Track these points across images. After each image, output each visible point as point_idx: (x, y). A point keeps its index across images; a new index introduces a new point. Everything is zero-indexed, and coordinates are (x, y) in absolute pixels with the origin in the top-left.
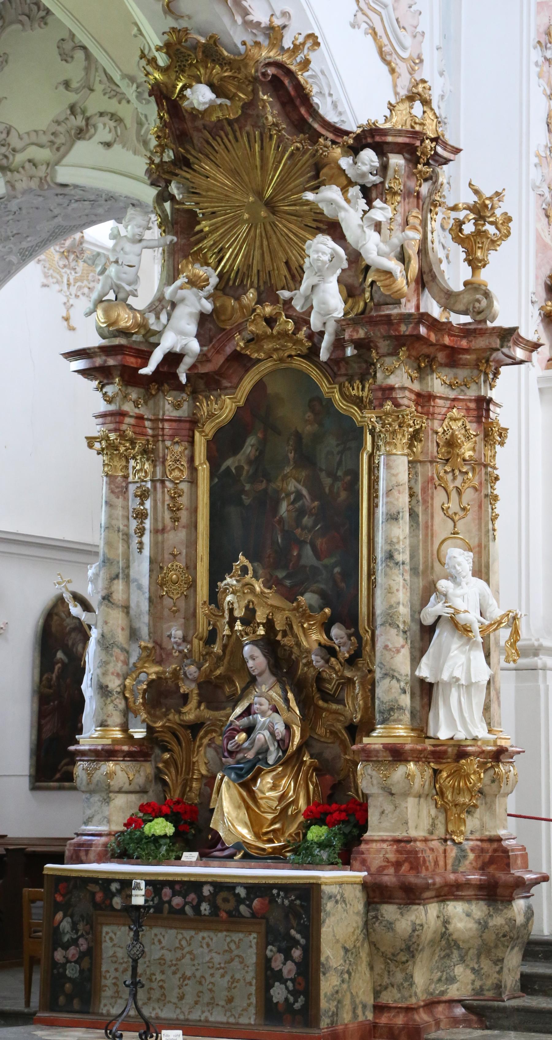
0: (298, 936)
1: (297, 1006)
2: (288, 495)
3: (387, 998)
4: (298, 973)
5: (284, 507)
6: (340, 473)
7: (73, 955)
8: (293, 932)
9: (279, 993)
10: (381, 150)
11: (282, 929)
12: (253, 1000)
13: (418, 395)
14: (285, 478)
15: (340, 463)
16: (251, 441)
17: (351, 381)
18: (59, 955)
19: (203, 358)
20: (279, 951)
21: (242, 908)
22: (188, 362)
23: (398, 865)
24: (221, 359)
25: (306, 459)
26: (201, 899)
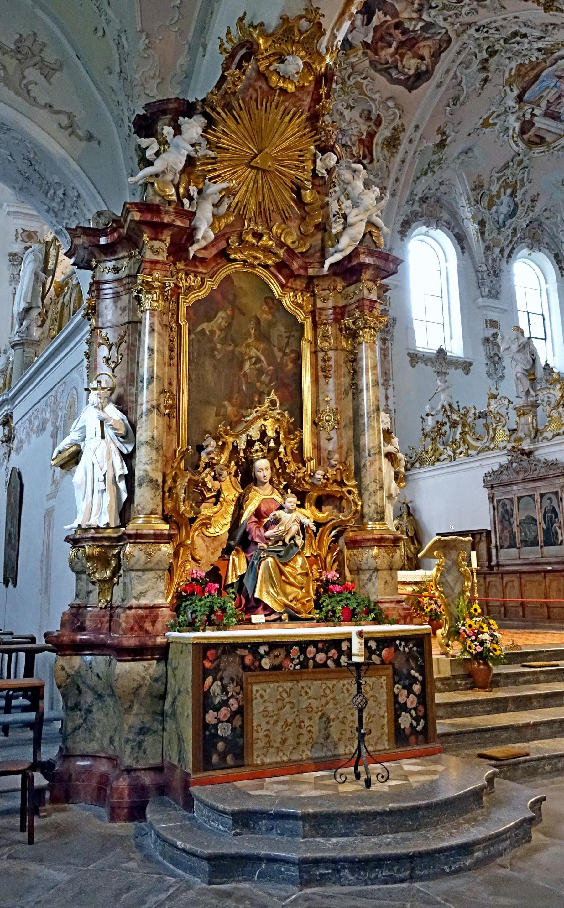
0: (417, 675)
6: (287, 351)
7: (225, 716)
8: (413, 672)
11: (405, 671)
15: (287, 344)
18: (210, 717)
20: (404, 687)
25: (263, 336)
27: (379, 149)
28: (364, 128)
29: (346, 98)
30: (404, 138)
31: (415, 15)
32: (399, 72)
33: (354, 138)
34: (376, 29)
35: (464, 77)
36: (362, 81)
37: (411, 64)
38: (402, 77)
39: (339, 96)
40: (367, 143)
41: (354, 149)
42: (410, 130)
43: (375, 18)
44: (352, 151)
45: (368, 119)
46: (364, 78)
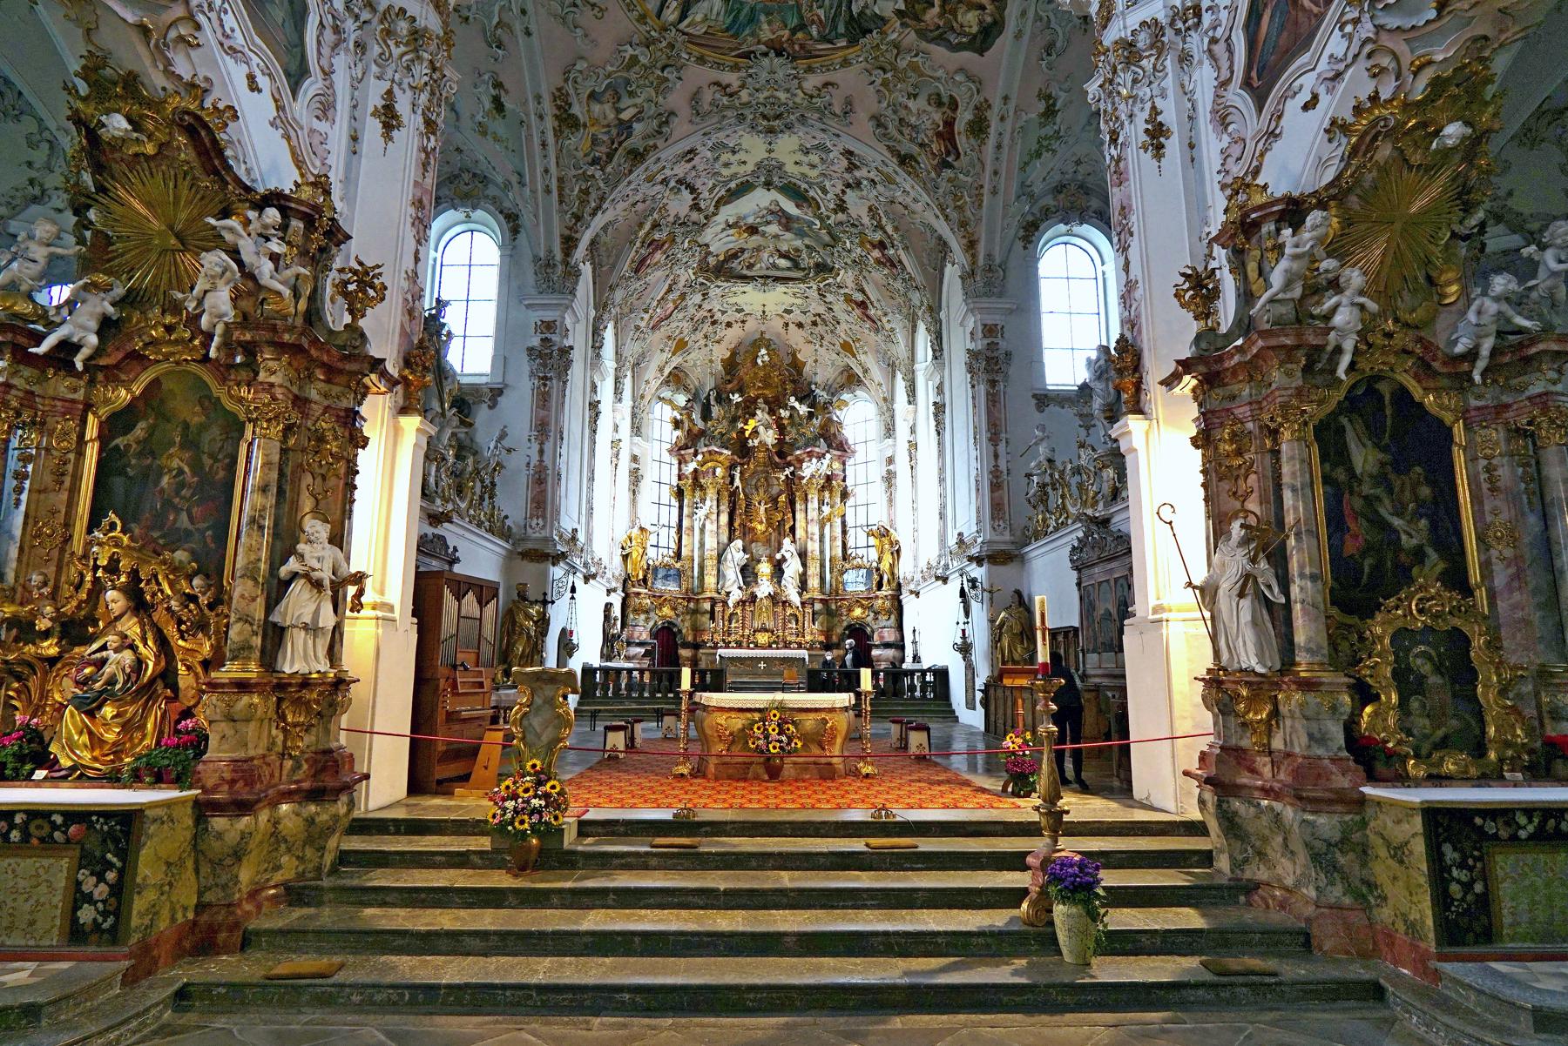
0: (115, 860)
1: (106, 926)
2: (170, 471)
3: (209, 897)
4: (111, 894)
5: (165, 480)
8: (109, 856)
9: (86, 914)
10: (284, 211)
11: (98, 854)
12: (58, 922)
13: (296, 397)
14: (171, 456)
16: (142, 425)
17: (238, 385)
19: (98, 352)
20: (92, 874)
21: (57, 835)
22: (85, 352)
23: (233, 782)
24: (120, 355)
25: (190, 443)
26: (12, 826)
27: (964, 139)
28: (938, 117)
30: (993, 117)
33: (930, 133)
40: (947, 134)
42: (997, 103)
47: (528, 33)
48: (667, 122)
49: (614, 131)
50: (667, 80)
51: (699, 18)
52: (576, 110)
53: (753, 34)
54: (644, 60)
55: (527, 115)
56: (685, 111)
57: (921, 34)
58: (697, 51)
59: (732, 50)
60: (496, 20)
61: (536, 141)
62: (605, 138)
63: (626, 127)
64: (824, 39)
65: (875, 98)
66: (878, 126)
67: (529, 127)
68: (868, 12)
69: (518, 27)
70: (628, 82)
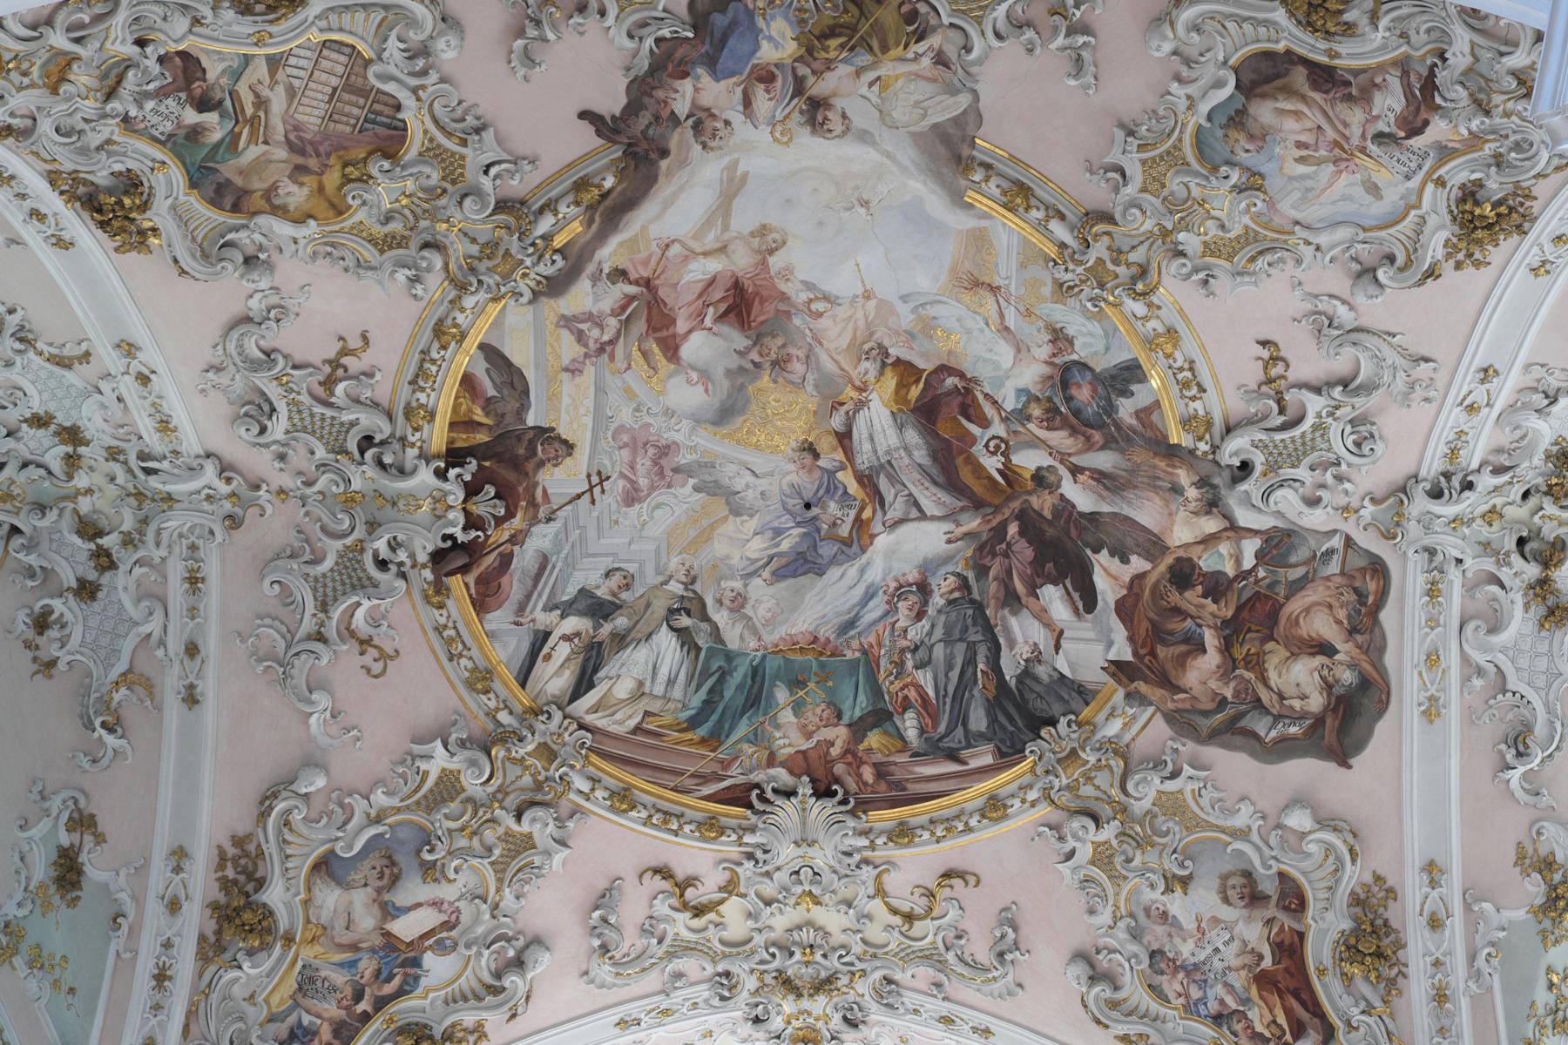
27: (1336, 986)
28: (1254, 932)
29: (1151, 857)
30: (1409, 916)
31: (1211, 525)
32: (1278, 718)
33: (1238, 980)
34: (1124, 610)
35: (1501, 659)
36: (1171, 786)
37: (1299, 679)
38: (1293, 730)
39: (1129, 861)
41: (1254, 1014)
42: (1413, 888)
43: (1100, 581)
44: (1250, 1027)
45: (1254, 898)
46: (1174, 775)
47: (191, 698)
48: (519, 963)
49: (367, 966)
50: (528, 843)
51: (623, 689)
52: (275, 895)
53: (755, 738)
54: (472, 783)
55: (138, 900)
56: (571, 942)
57: (1182, 722)
58: (616, 776)
59: (705, 779)
60: (122, 666)
61: (145, 967)
62: (340, 978)
63: (402, 960)
64: (936, 749)
65: (1080, 901)
66: (1093, 979)
67: (134, 932)
68: (1042, 671)
69: (171, 684)
70: (427, 839)
